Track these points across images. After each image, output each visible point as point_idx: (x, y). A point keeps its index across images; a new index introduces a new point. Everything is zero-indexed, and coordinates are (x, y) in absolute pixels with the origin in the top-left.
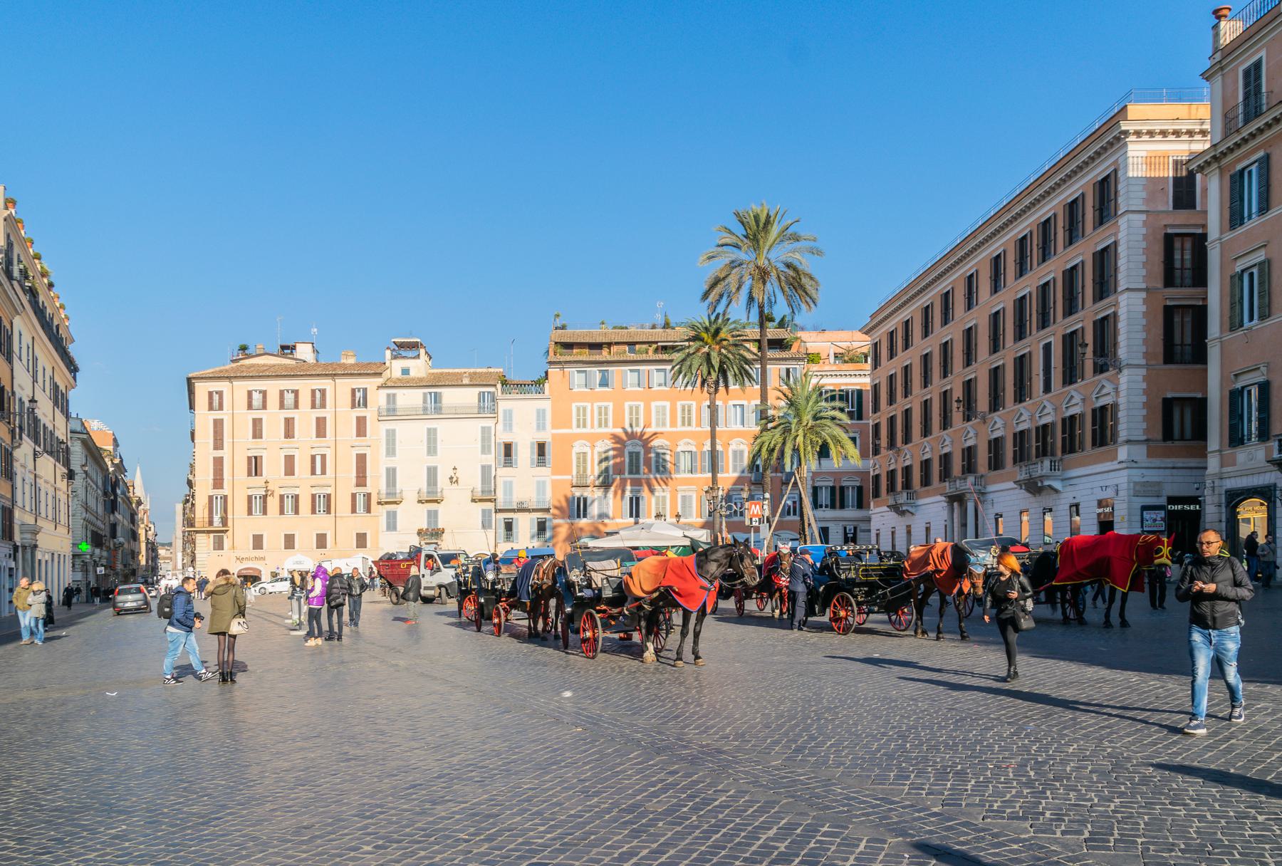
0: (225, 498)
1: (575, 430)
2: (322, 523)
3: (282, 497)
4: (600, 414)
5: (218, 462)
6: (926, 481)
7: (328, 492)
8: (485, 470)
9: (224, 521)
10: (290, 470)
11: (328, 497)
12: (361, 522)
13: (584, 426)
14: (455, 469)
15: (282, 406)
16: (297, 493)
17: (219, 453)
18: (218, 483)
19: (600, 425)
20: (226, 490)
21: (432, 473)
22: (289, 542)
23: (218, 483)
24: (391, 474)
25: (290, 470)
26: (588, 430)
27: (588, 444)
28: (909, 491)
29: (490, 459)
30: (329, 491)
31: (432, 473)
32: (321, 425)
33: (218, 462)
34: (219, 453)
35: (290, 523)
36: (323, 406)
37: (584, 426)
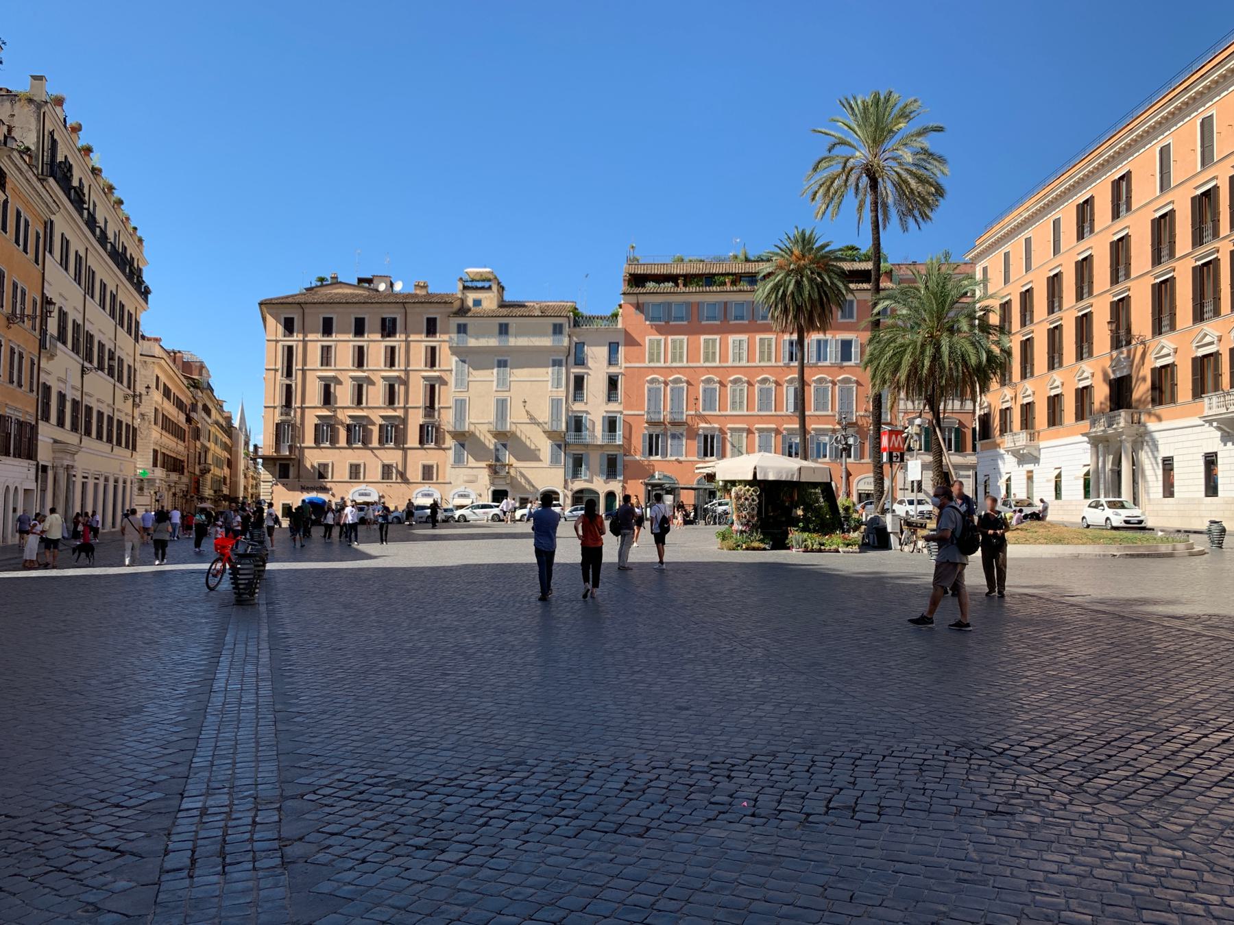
1: (647, 364)
2: (392, 456)
4: (674, 348)
6: (1054, 419)
8: (555, 403)
12: (430, 456)
13: (659, 361)
14: (525, 402)
19: (673, 360)
21: (502, 405)
22: (355, 471)
24: (461, 406)
26: (662, 364)
27: (662, 379)
28: (1032, 431)
29: (561, 393)
31: (502, 405)
32: (391, 352)
35: (357, 456)
37: (659, 361)
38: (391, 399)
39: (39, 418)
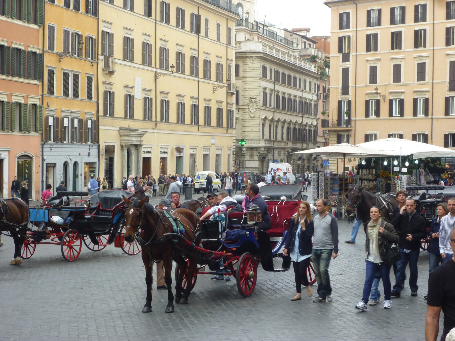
0: (349, 102)
3: (391, 101)
5: (346, 72)
7: (427, 97)
9: (348, 122)
10: (397, 77)
11: (426, 101)
15: (393, 22)
16: (402, 98)
17: (346, 65)
18: (345, 90)
20: (351, 97)
23: (345, 90)
25: (397, 77)
30: (427, 96)
33: (346, 72)
34: (346, 65)
36: (424, 19)
38: (421, 76)
39: (101, 113)
